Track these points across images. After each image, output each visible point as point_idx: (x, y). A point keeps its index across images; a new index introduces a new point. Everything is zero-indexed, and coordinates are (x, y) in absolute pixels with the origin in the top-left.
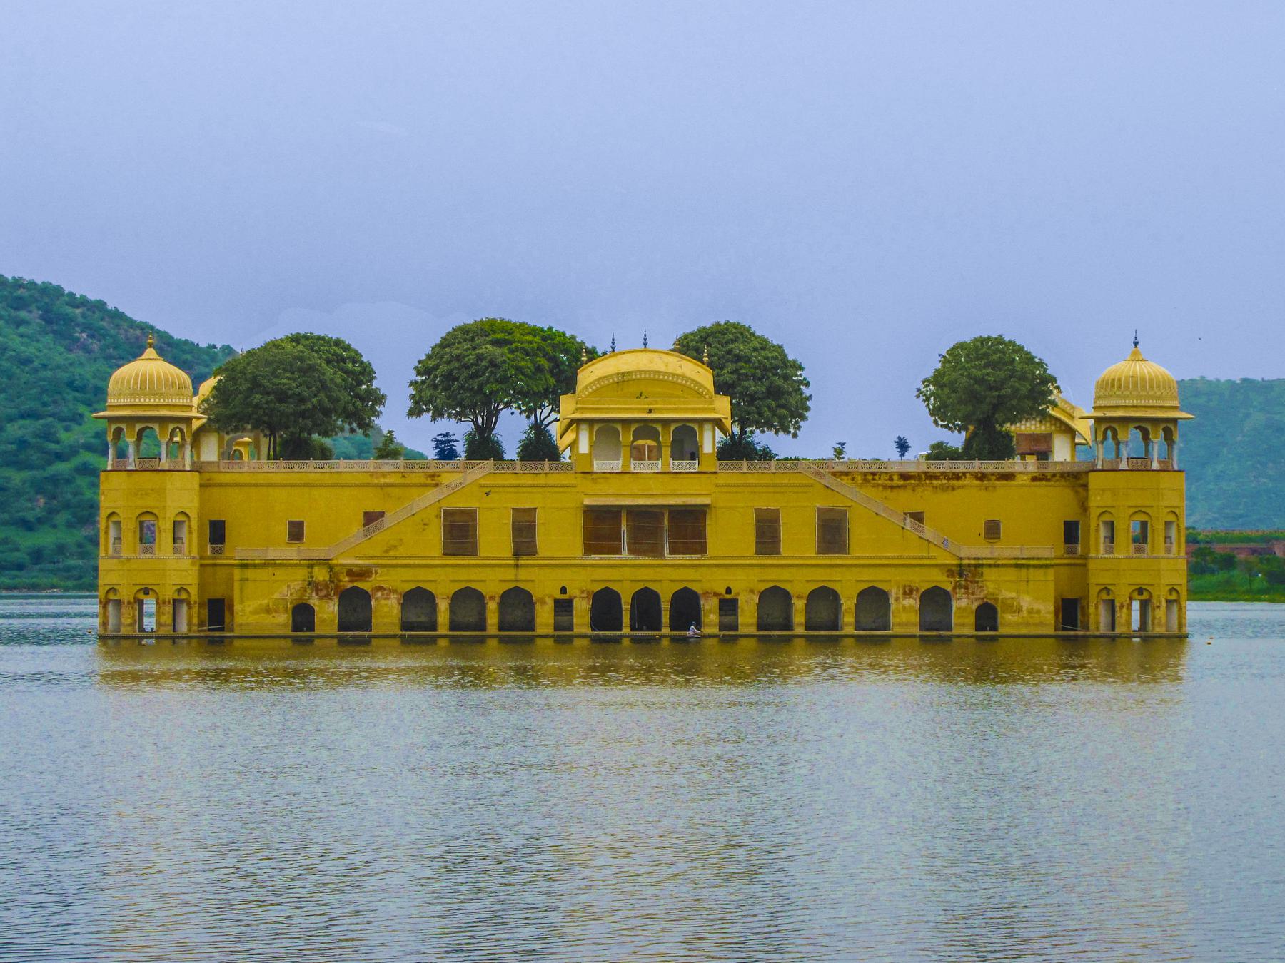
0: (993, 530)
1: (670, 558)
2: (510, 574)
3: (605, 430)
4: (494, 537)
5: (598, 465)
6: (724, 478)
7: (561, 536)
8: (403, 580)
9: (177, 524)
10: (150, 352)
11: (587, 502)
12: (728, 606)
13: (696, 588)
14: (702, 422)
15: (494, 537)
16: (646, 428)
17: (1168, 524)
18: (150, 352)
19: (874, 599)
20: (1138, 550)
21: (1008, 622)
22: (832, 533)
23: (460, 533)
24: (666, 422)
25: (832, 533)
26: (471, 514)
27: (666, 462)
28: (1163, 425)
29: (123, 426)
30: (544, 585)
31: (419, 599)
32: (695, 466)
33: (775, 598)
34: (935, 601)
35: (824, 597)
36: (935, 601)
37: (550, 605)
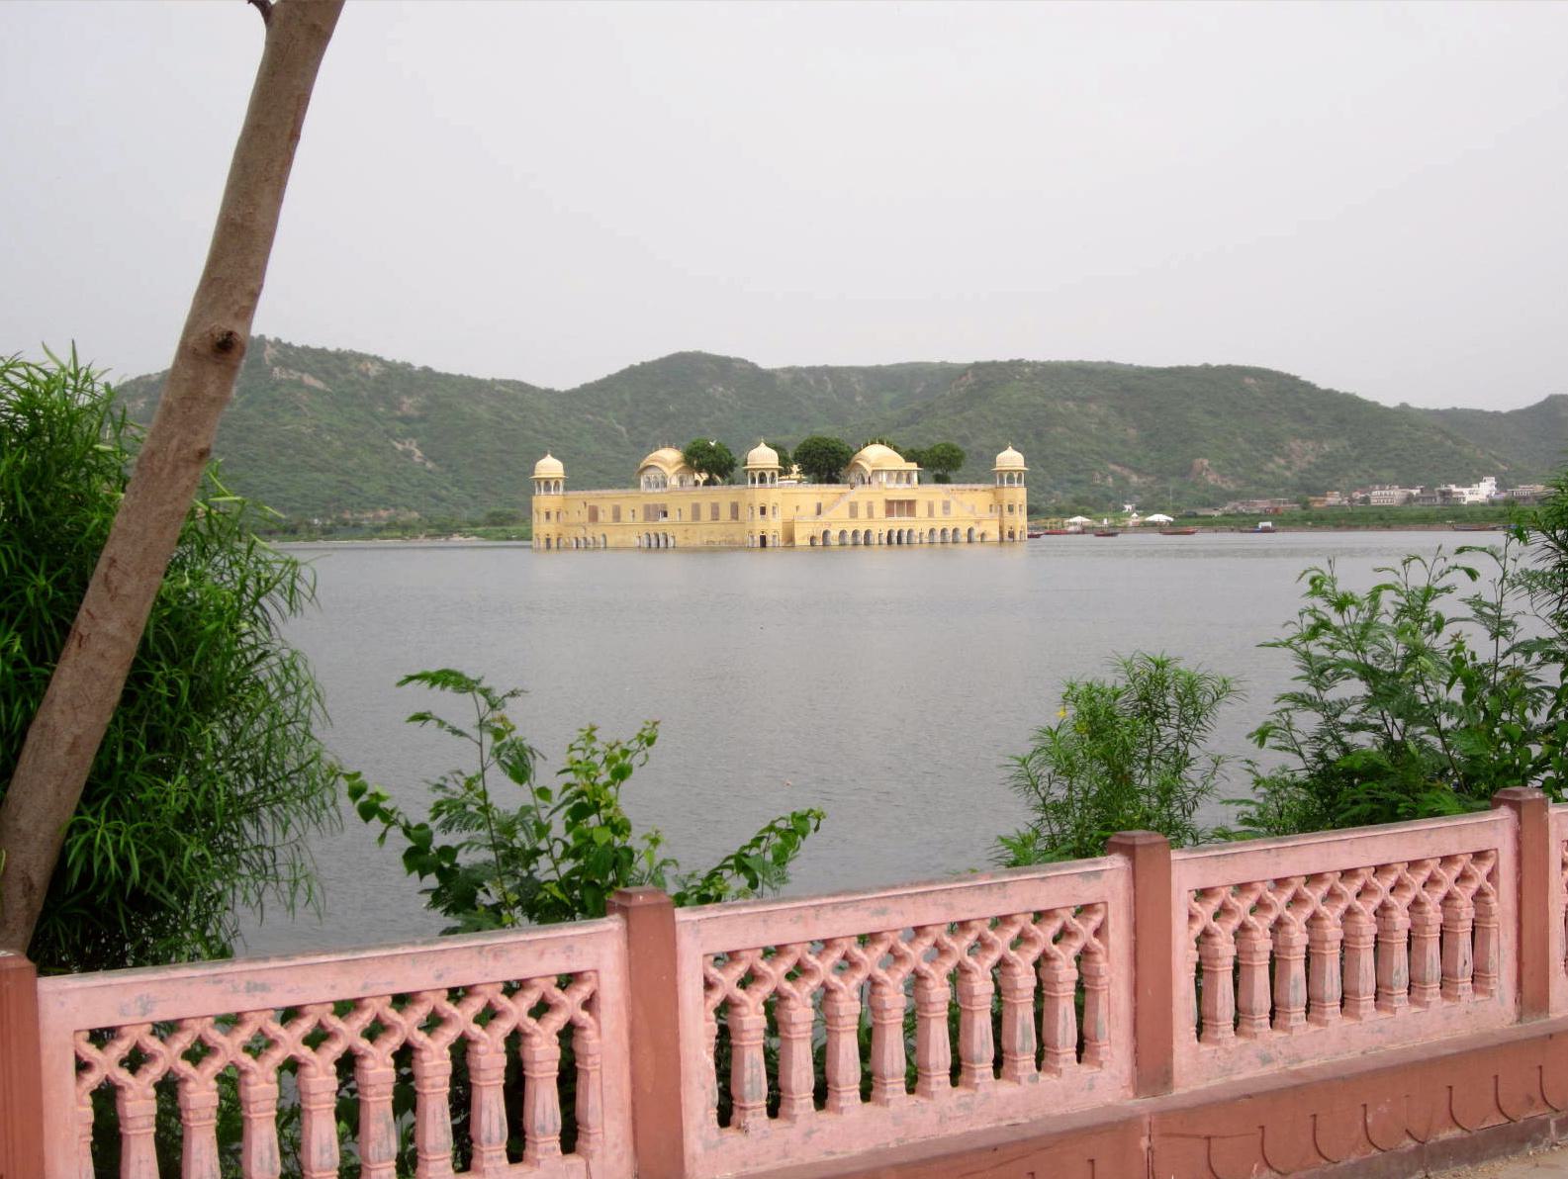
1: (906, 518)
3: (890, 472)
5: (888, 486)
7: (880, 510)
10: (762, 444)
11: (890, 499)
15: (862, 512)
16: (899, 473)
18: (762, 444)
21: (988, 539)
22: (946, 507)
23: (853, 511)
25: (946, 507)
26: (856, 503)
27: (904, 485)
33: (932, 531)
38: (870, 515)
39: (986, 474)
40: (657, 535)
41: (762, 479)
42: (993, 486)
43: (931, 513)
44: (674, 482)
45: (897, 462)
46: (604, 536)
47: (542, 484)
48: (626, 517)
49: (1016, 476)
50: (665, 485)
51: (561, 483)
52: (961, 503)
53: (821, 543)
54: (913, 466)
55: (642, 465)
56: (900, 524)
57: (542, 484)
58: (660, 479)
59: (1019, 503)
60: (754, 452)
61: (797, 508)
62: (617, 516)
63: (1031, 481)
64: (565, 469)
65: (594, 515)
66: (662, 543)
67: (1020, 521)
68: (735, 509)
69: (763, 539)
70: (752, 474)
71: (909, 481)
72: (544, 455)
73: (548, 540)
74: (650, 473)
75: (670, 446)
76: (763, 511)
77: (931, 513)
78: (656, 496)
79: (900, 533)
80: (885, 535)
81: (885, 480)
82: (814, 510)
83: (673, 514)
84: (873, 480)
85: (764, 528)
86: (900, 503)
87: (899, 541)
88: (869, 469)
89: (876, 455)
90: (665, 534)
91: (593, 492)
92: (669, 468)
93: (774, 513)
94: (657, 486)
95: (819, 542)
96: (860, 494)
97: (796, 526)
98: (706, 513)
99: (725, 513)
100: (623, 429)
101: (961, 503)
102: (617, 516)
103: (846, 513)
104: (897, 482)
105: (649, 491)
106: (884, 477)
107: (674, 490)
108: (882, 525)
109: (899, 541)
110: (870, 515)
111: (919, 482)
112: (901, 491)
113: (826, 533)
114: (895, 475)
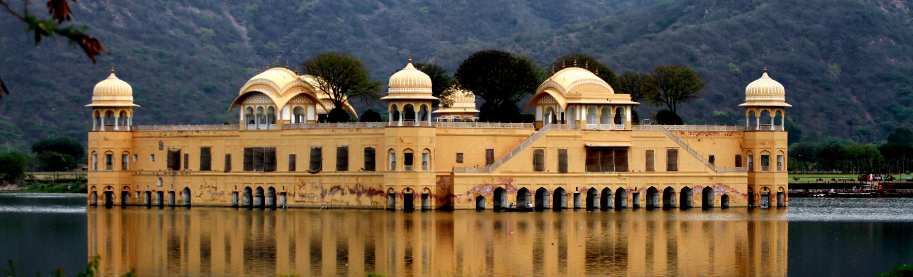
0: (712, 159)
2: (557, 181)
4: (551, 163)
5: (588, 126)
6: (634, 134)
7: (577, 162)
8: (518, 184)
9: (424, 154)
11: (589, 144)
12: (635, 195)
13: (624, 187)
14: (626, 105)
15: (551, 163)
16: (605, 107)
17: (779, 156)
19: (685, 192)
20: (764, 169)
21: (731, 203)
24: (613, 105)
27: (612, 125)
28: (761, 110)
29: (397, 104)
30: (570, 185)
31: (522, 193)
32: (622, 127)
33: (651, 192)
34: (707, 192)
35: (668, 192)
36: (707, 192)
37: (572, 196)
38: (563, 167)
39: (732, 112)
40: (260, 189)
41: (409, 115)
42: (742, 128)
43: (650, 166)
44: (287, 115)
45: (604, 93)
46: (188, 190)
47: (103, 115)
48: (218, 163)
49: (773, 114)
50: (274, 121)
51: (129, 115)
52: (695, 154)
53: (496, 204)
54: (625, 98)
55: (242, 91)
56: (606, 181)
57: (103, 115)
58: (266, 113)
59: (776, 153)
60: (399, 77)
61: (460, 158)
62: (206, 164)
63: (793, 119)
64: (135, 95)
65: (175, 161)
66: (268, 201)
67: (779, 179)
68: (370, 156)
69: (409, 199)
70: (394, 107)
71: (618, 120)
72: (105, 76)
73: (109, 194)
74: (254, 102)
75: (282, 65)
76: (409, 159)
77: (650, 166)
78: (258, 137)
79: (606, 192)
80: (583, 197)
81: (584, 118)
82: (482, 160)
83: (282, 164)
84: (567, 118)
85: (408, 183)
86: (606, 150)
87: (605, 207)
88: (562, 102)
89: (573, 81)
90: (272, 189)
91: (175, 128)
92: (279, 96)
93: (424, 163)
94: (263, 122)
95: (488, 204)
96: (550, 139)
97: (456, 181)
98: (329, 161)
99: (356, 161)
100: (243, 30)
101: (695, 154)
102: (206, 164)
103: (530, 166)
104: (602, 122)
105: (251, 127)
106: (583, 114)
107: (287, 126)
108: (580, 179)
109: (605, 207)
110: (563, 167)
111: (635, 120)
112: (607, 135)
113: (498, 193)
114: (598, 112)
